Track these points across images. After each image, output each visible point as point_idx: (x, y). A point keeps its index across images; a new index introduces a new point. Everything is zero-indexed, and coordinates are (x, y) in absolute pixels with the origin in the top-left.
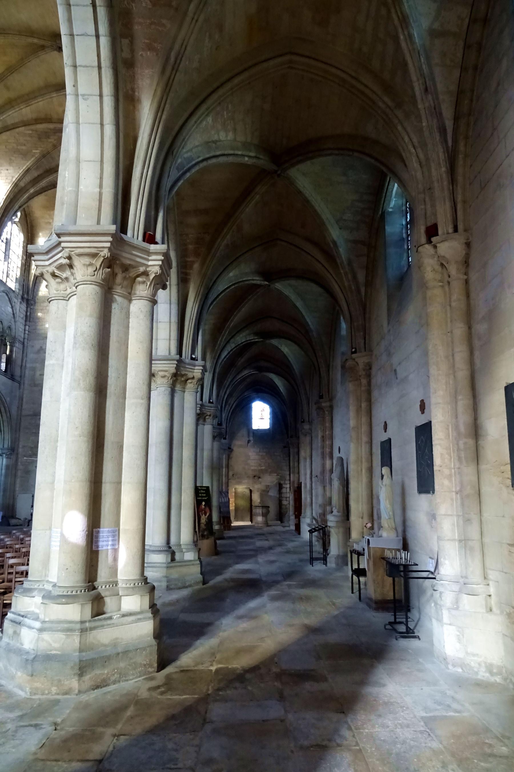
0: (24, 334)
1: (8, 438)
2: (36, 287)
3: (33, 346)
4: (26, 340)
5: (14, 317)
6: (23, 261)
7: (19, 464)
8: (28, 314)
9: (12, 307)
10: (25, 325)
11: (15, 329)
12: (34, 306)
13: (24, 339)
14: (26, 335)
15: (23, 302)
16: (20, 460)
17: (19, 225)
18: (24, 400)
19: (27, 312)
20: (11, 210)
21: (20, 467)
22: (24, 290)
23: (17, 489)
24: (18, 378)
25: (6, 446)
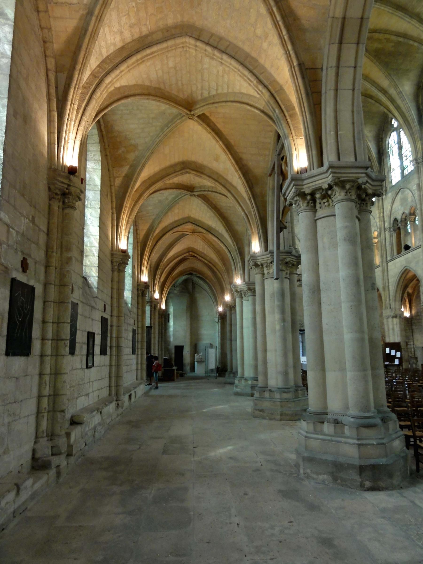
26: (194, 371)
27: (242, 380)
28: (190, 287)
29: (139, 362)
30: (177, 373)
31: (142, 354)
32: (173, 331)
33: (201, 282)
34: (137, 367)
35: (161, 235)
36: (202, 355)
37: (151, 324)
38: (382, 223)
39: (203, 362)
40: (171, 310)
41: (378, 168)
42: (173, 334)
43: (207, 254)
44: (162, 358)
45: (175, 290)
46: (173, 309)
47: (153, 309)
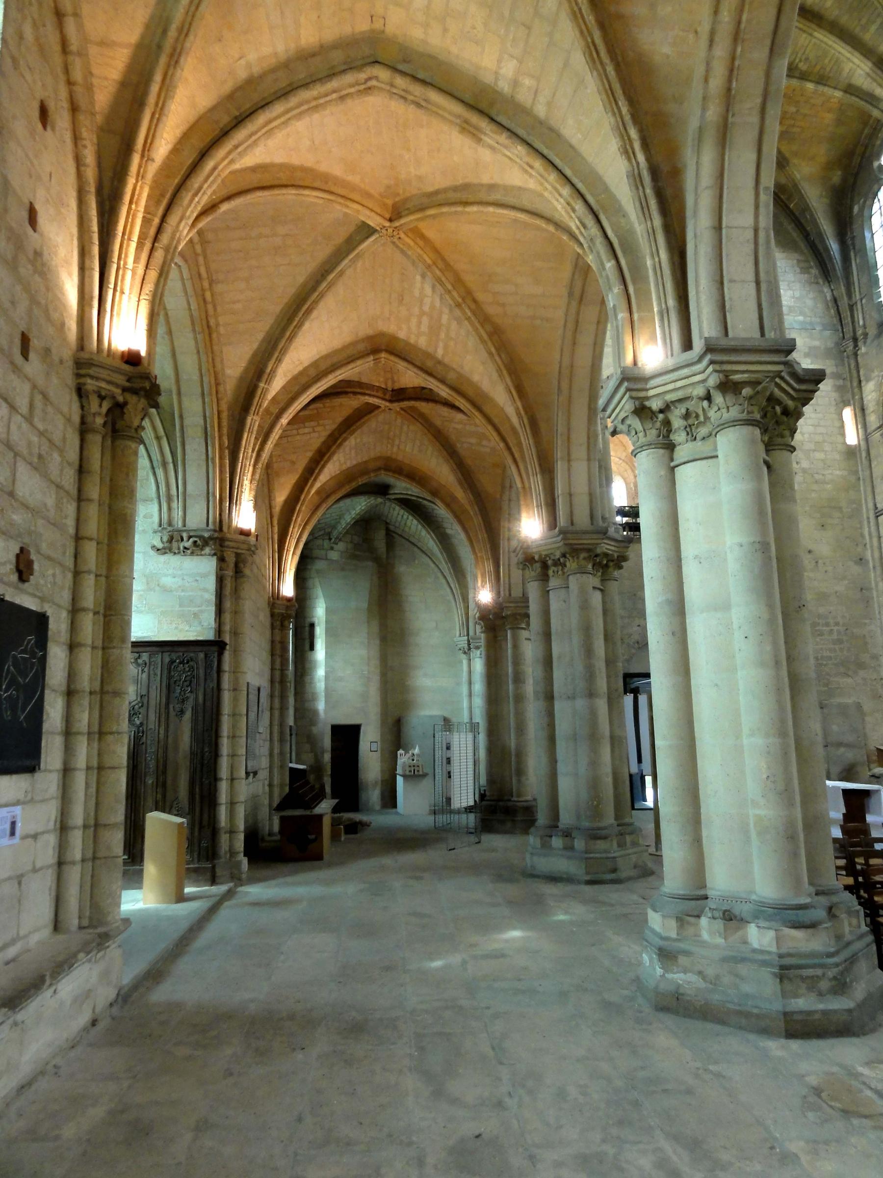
26: (395, 806)
27: (551, 836)
28: (380, 543)
29: (78, 816)
30: (335, 823)
31: (101, 769)
32: (327, 677)
33: (412, 525)
34: (62, 847)
35: (225, 119)
36: (418, 755)
37: (219, 631)
39: (425, 775)
40: (320, 612)
42: (326, 688)
43: (446, 360)
44: (282, 767)
45: (332, 548)
46: (327, 608)
47: (229, 572)
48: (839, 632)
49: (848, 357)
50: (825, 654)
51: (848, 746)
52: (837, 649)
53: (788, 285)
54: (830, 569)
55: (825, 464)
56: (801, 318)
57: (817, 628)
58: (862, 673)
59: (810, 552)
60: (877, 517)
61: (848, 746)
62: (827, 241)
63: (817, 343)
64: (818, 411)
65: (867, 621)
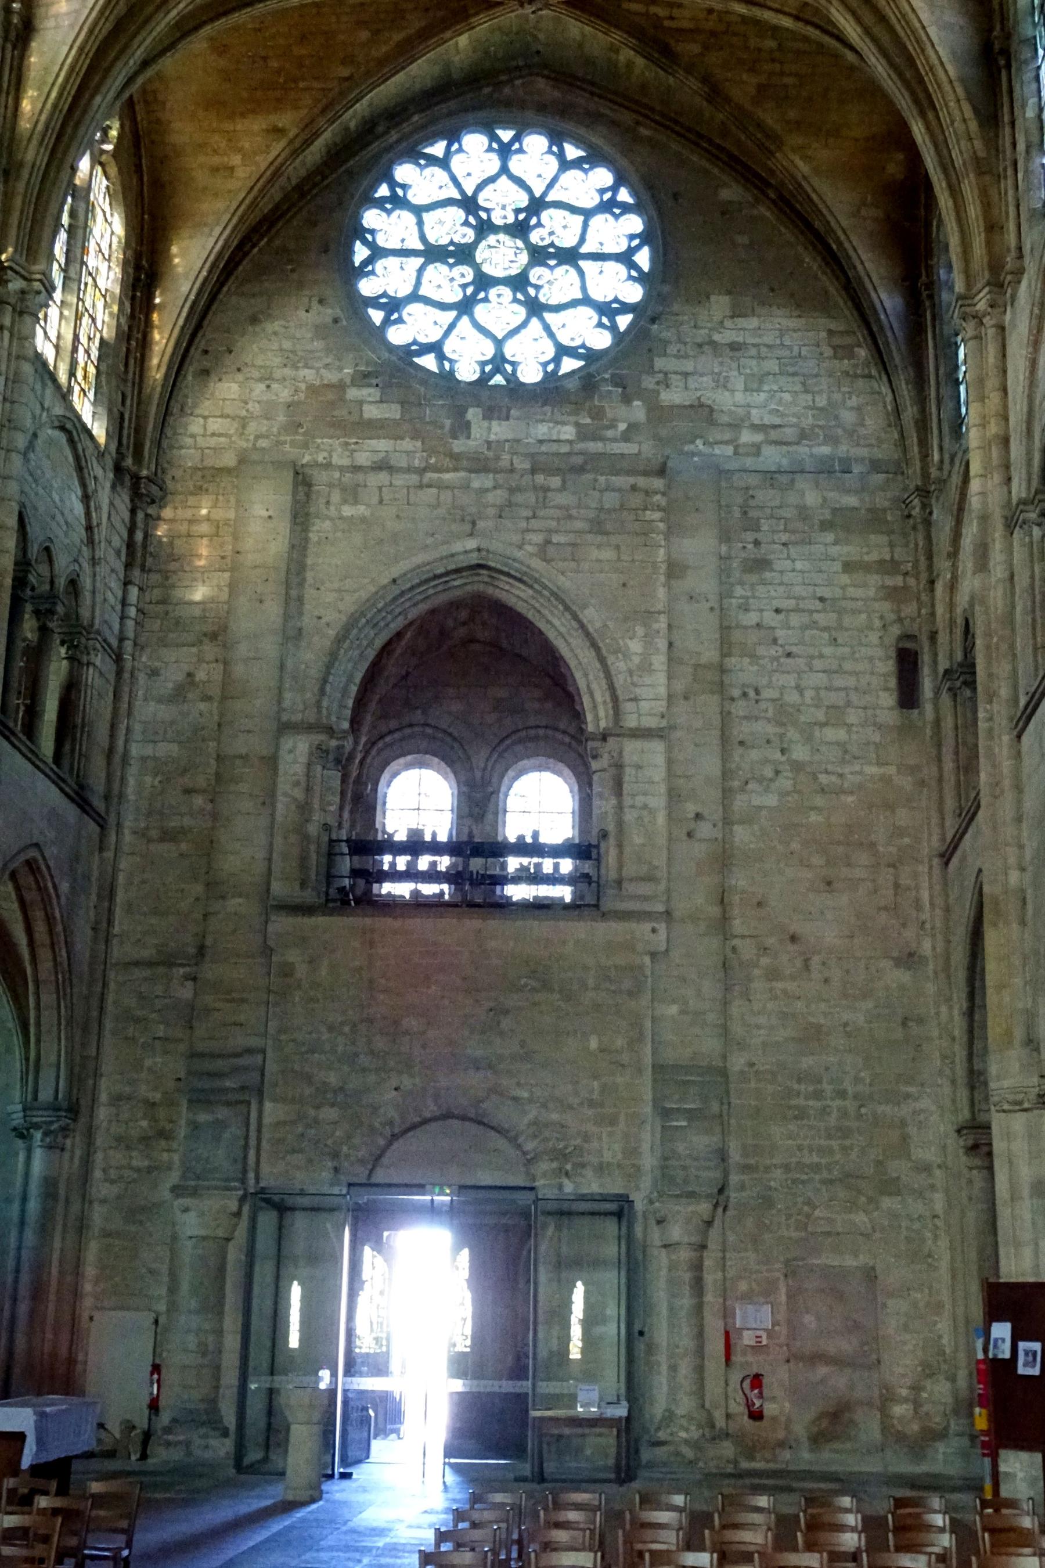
0: (123, 618)
1: (53, 1058)
2: (169, 432)
3: (154, 673)
4: (128, 645)
5: (91, 542)
6: (123, 321)
7: (98, 1174)
8: (139, 536)
9: (86, 498)
10: (127, 583)
11: (94, 592)
12: (161, 507)
13: (122, 639)
14: (130, 624)
15: (122, 484)
16: (99, 1156)
17: (113, 170)
18: (120, 897)
19: (131, 531)
20: (119, 64)
21: (101, 1188)
22: (125, 441)
23: (88, 1287)
24: (99, 804)
25: (45, 1095)
38: (997, 478)
41: (978, 144)
48: (844, 1114)
49: (914, 528)
50: (807, 1160)
51: (838, 1362)
52: (836, 1148)
53: (804, 384)
54: (836, 974)
55: (846, 752)
56: (825, 450)
57: (793, 1102)
58: (887, 1202)
59: (793, 939)
60: (947, 864)
61: (838, 1362)
62: (873, 295)
63: (852, 501)
64: (840, 641)
65: (912, 1090)
